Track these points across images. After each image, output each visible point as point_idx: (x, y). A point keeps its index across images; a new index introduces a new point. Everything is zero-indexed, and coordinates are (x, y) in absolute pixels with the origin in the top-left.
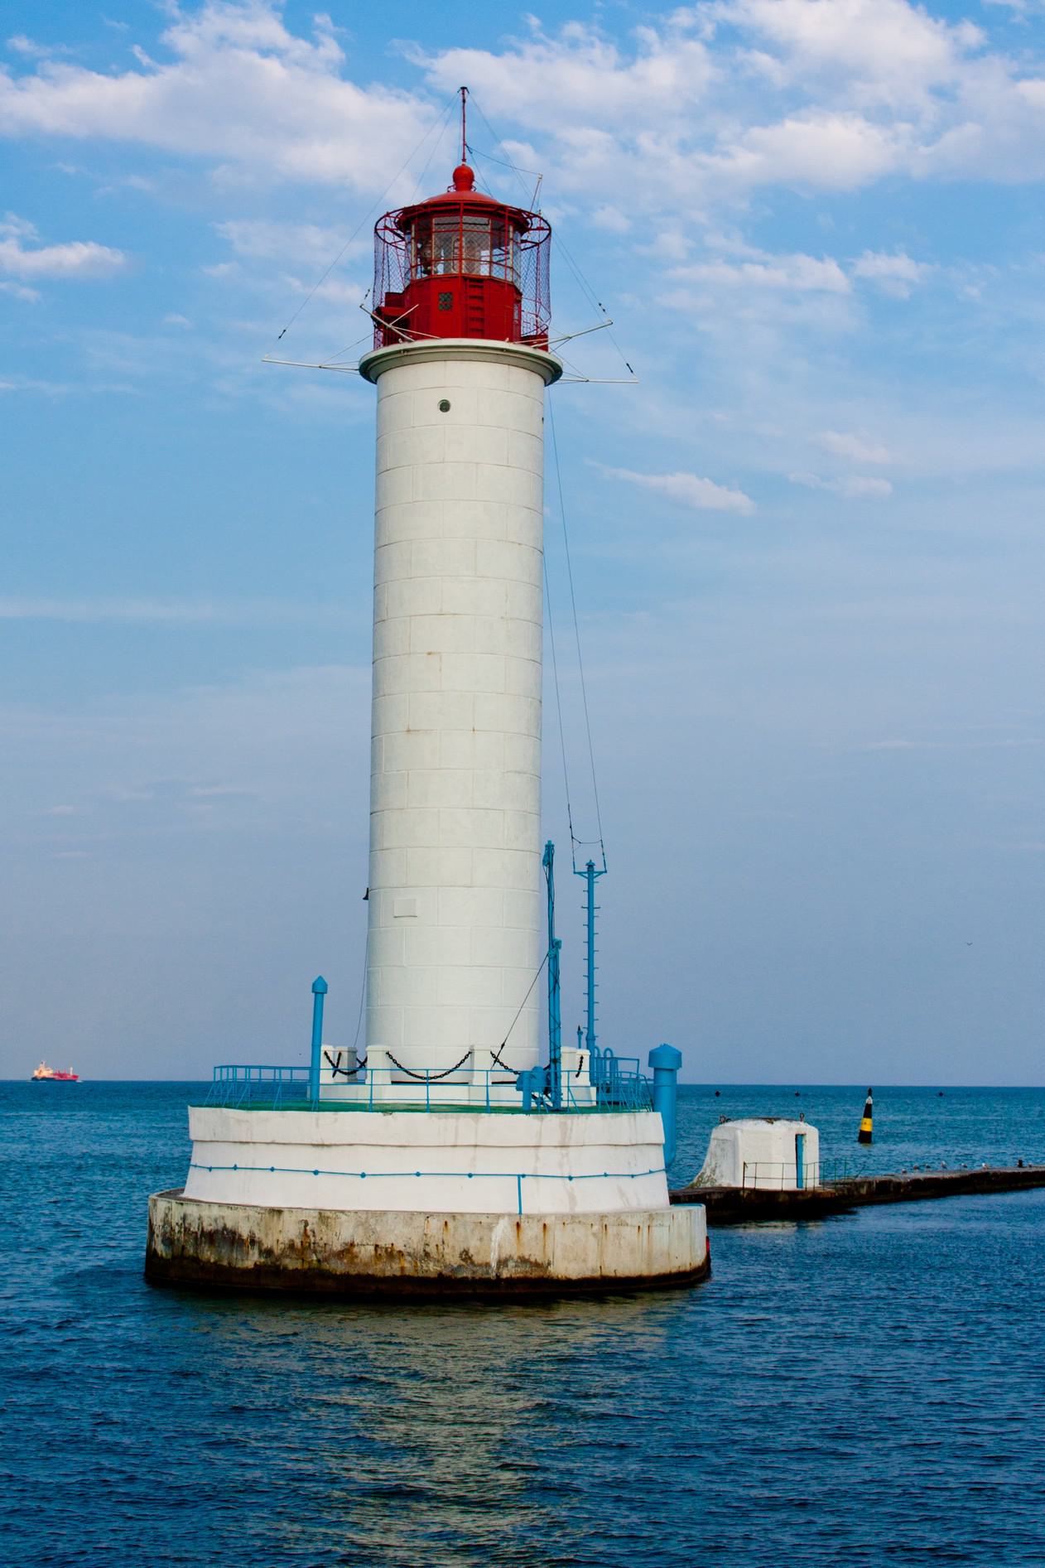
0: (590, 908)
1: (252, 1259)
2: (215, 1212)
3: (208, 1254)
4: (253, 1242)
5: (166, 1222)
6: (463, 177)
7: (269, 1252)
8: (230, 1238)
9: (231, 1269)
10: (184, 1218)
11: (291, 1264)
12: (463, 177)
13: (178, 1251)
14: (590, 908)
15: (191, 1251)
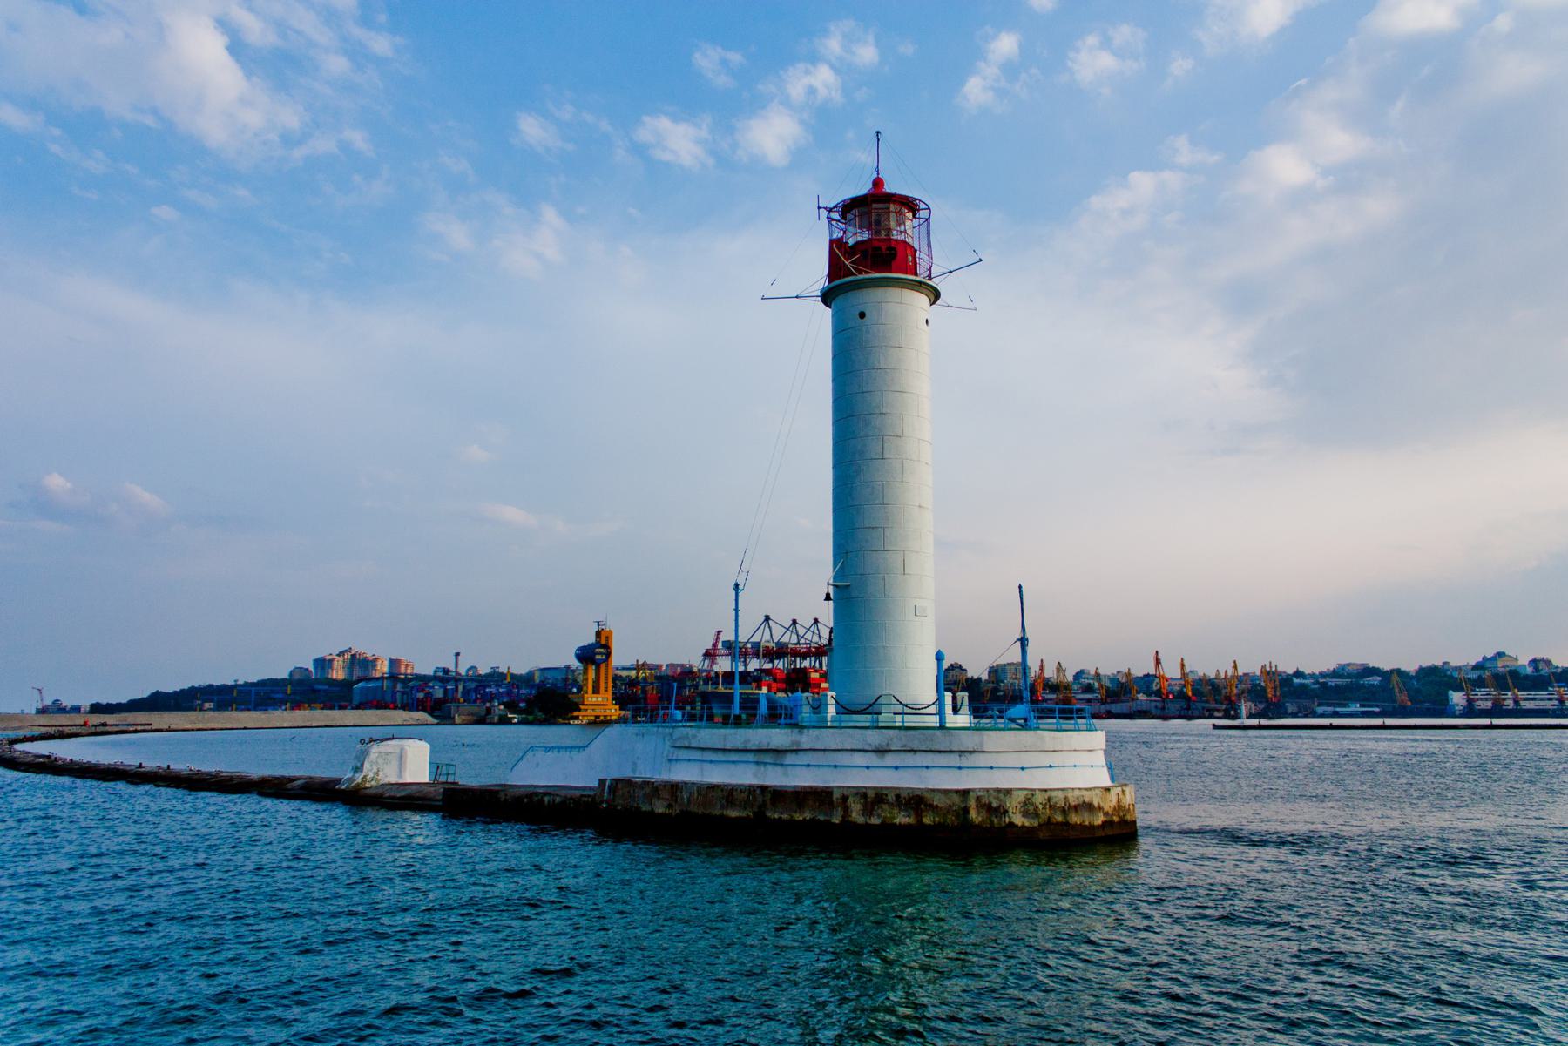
0: (737, 610)
1: (1099, 819)
2: (1077, 793)
3: (1075, 819)
4: (1100, 808)
5: (1028, 801)
6: (878, 183)
7: (1106, 814)
8: (1089, 807)
9: (1092, 827)
10: (1049, 799)
11: (1116, 819)
12: (878, 183)
13: (1043, 819)
14: (737, 610)
15: (1060, 818)
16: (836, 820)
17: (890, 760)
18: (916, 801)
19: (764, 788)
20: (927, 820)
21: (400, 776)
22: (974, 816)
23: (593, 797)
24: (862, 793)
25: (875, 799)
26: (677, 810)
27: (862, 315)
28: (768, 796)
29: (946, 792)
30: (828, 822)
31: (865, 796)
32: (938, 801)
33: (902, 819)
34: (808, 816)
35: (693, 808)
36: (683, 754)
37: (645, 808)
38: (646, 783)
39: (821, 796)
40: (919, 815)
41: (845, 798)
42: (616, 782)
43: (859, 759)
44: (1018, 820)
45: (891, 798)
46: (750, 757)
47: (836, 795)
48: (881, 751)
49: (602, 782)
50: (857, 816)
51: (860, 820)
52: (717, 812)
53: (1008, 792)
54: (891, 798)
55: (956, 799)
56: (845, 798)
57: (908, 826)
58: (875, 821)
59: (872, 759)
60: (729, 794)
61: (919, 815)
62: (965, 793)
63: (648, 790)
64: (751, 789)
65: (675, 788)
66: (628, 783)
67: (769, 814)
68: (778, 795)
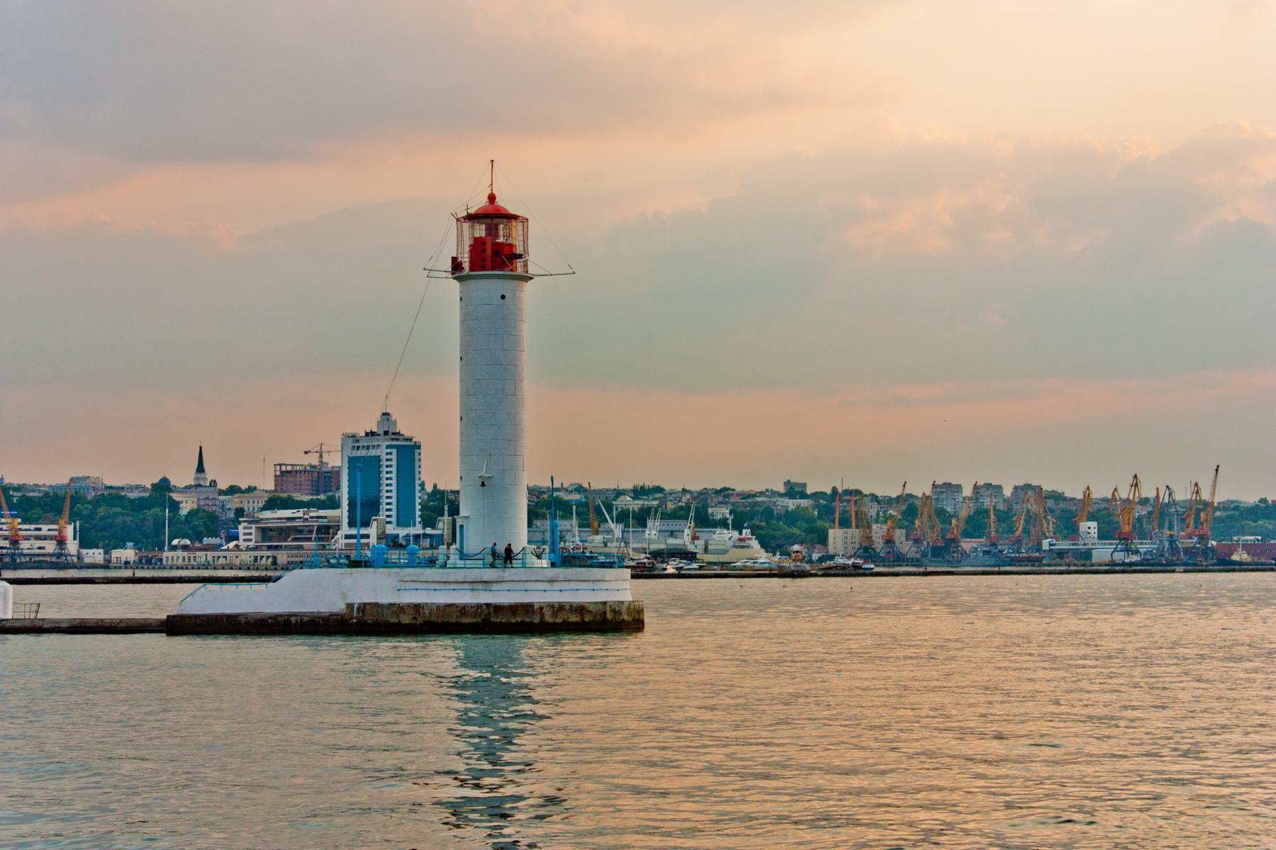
5: (629, 608)
6: (492, 198)
12: (492, 198)
16: (537, 620)
17: (557, 586)
18: (581, 609)
19: (488, 605)
20: (587, 619)
21: (5, 613)
22: (609, 616)
23: (343, 616)
24: (552, 606)
25: (559, 608)
26: (420, 620)
27: (503, 297)
28: (492, 610)
29: (596, 603)
30: (532, 623)
31: (553, 606)
32: (592, 608)
33: (574, 618)
34: (519, 619)
35: (433, 619)
36: (408, 586)
37: (394, 620)
38: (391, 605)
39: (528, 608)
40: (582, 615)
41: (541, 608)
42: (365, 604)
43: (539, 586)
44: (626, 617)
45: (567, 607)
46: (466, 586)
47: (536, 607)
48: (551, 581)
49: (350, 606)
50: (548, 618)
51: (551, 620)
52: (454, 620)
53: (622, 602)
54: (567, 607)
55: (601, 606)
56: (541, 608)
57: (576, 623)
58: (559, 620)
59: (546, 586)
60: (463, 609)
61: (582, 615)
62: (605, 603)
63: (395, 609)
64: (479, 606)
65: (417, 607)
66: (377, 605)
67: (493, 620)
68: (498, 608)
